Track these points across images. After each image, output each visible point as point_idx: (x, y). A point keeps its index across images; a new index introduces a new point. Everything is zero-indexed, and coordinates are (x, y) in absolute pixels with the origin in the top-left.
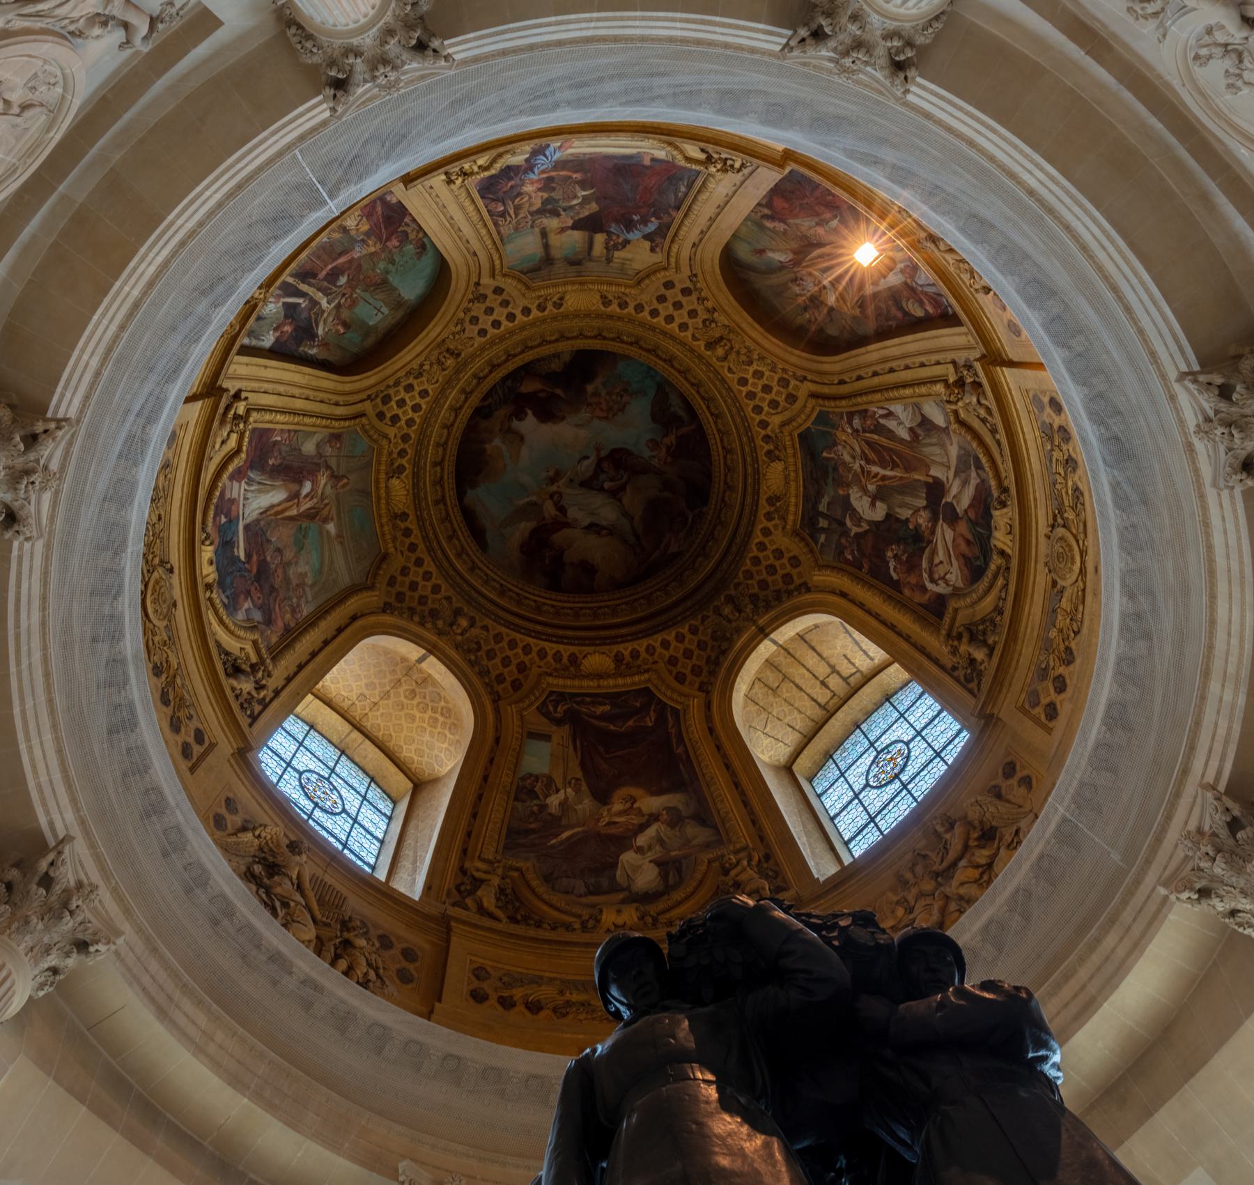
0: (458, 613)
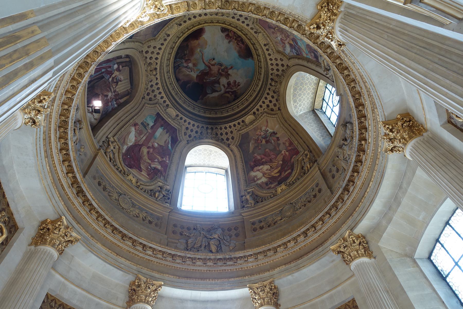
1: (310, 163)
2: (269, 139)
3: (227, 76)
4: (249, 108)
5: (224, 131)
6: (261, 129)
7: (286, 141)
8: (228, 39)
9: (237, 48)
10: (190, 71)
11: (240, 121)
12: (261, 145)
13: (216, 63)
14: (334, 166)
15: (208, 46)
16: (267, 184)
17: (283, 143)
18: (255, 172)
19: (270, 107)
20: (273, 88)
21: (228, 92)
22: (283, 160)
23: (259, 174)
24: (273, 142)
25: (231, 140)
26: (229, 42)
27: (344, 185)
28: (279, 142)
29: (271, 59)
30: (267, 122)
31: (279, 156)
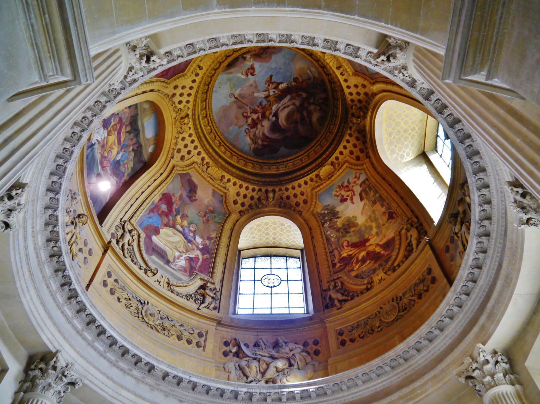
0: (267, 191)
25: (302, 204)
29: (348, 87)
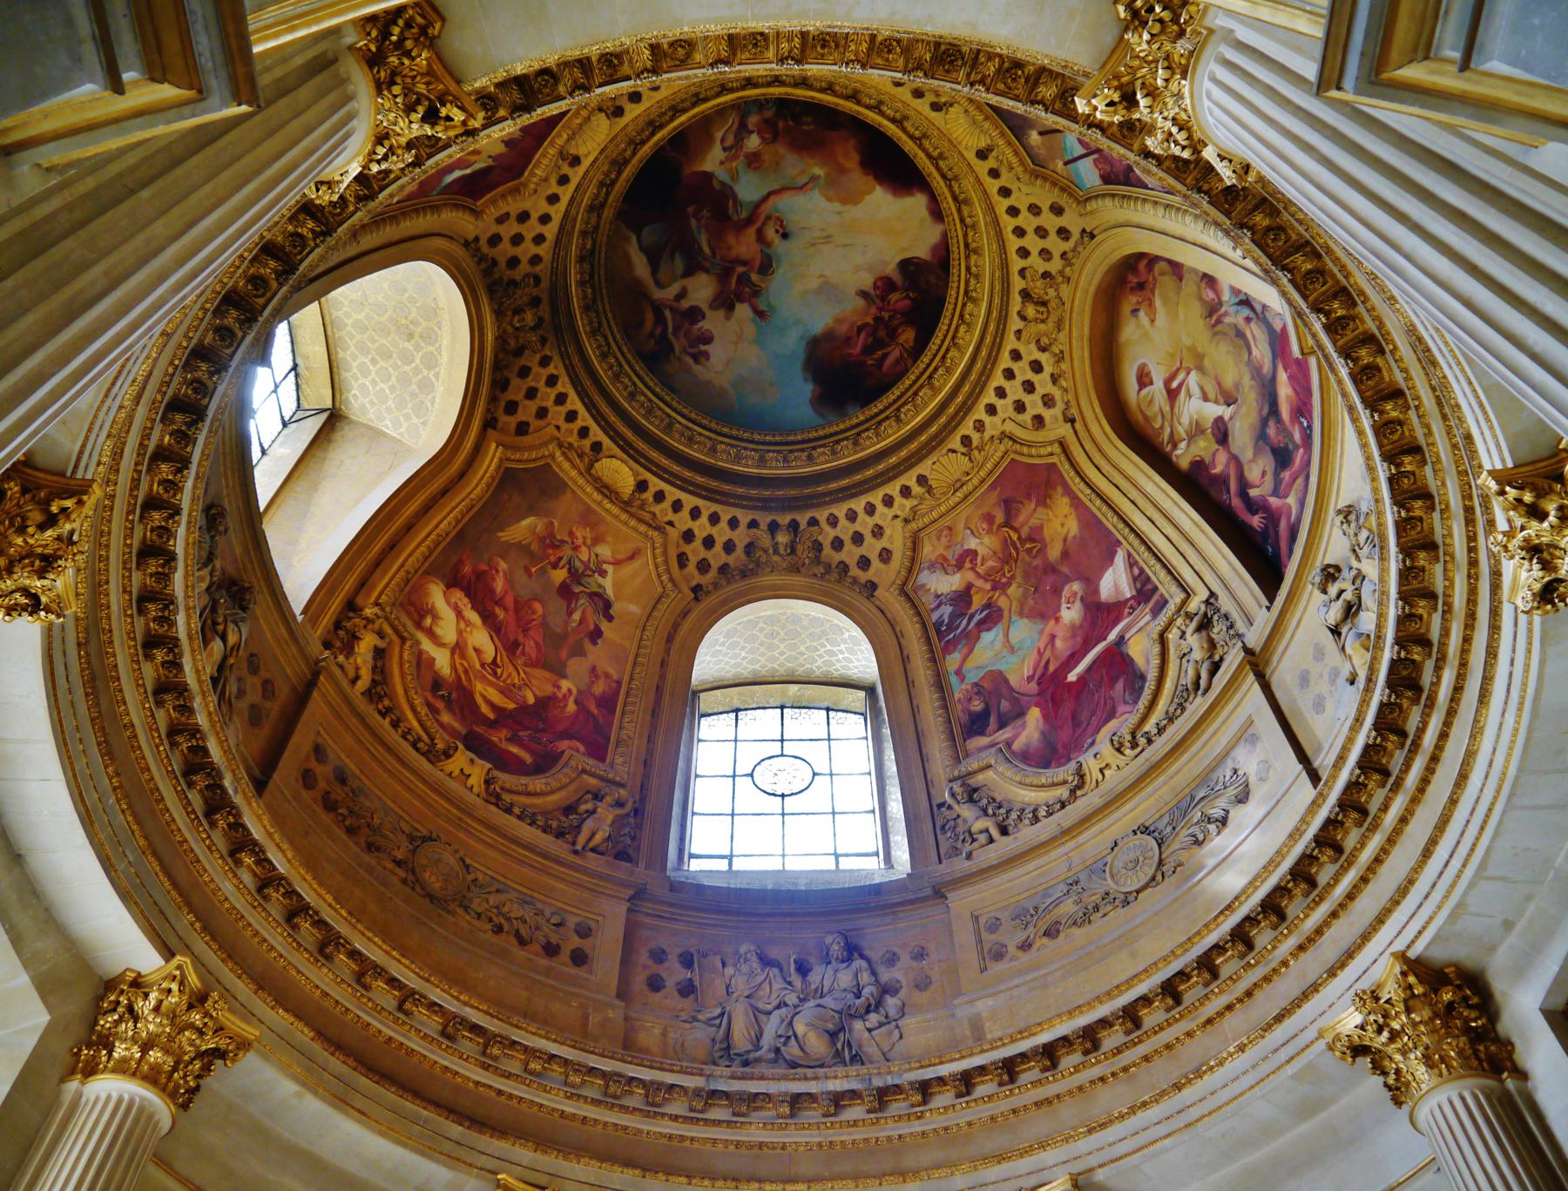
1: (608, 839)
2: (576, 596)
3: (725, 302)
4: (654, 454)
5: (537, 379)
6: (597, 540)
7: (607, 675)
8: (875, 286)
9: (843, 329)
10: (728, 143)
11: (597, 434)
12: (543, 571)
13: (769, 245)
14: (687, 961)
15: (837, 206)
16: (437, 683)
17: (594, 669)
18: (448, 602)
19: (688, 549)
20: (765, 540)
21: (660, 319)
22: (544, 703)
23: (447, 628)
24: (577, 616)
25: (512, 421)
26: (863, 294)
27: (722, 1086)
28: (588, 645)
30: (631, 558)
31: (547, 675)
